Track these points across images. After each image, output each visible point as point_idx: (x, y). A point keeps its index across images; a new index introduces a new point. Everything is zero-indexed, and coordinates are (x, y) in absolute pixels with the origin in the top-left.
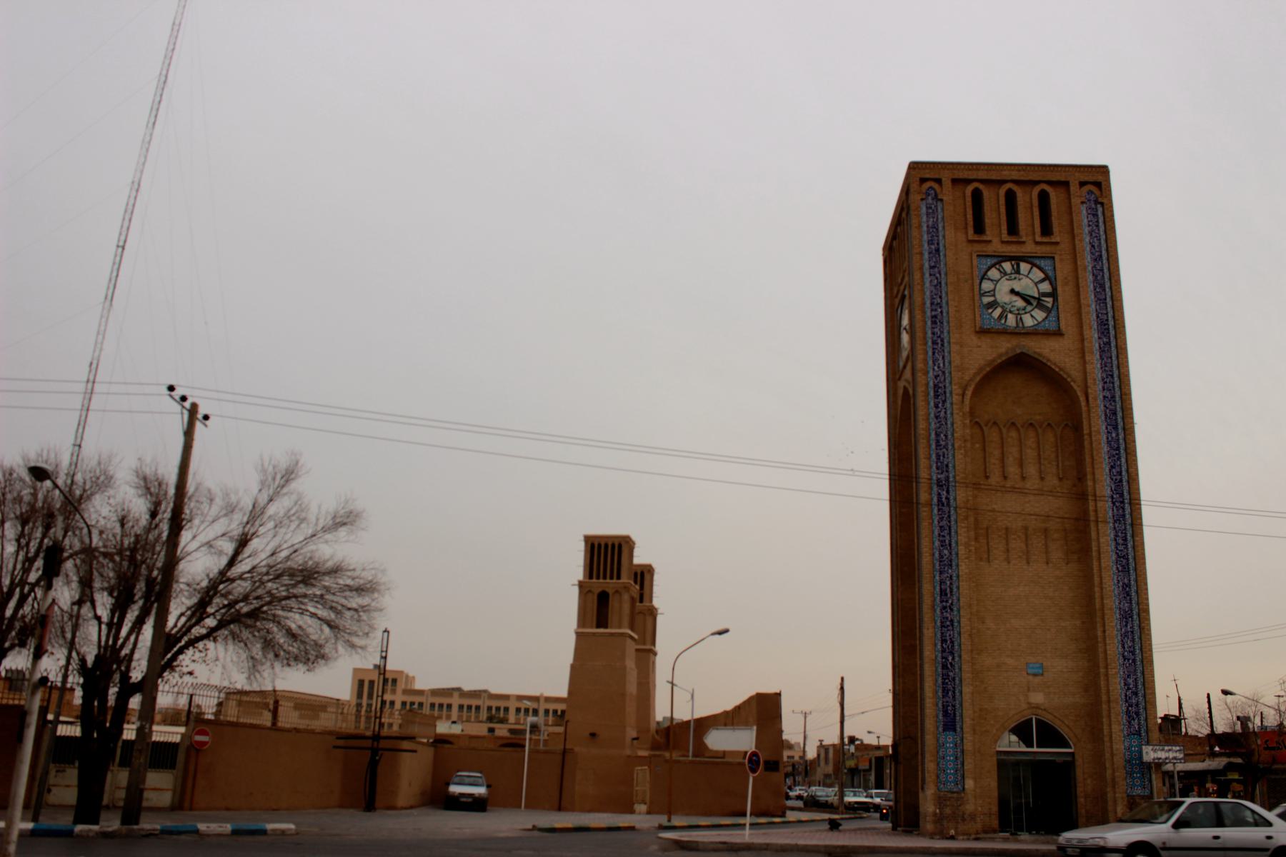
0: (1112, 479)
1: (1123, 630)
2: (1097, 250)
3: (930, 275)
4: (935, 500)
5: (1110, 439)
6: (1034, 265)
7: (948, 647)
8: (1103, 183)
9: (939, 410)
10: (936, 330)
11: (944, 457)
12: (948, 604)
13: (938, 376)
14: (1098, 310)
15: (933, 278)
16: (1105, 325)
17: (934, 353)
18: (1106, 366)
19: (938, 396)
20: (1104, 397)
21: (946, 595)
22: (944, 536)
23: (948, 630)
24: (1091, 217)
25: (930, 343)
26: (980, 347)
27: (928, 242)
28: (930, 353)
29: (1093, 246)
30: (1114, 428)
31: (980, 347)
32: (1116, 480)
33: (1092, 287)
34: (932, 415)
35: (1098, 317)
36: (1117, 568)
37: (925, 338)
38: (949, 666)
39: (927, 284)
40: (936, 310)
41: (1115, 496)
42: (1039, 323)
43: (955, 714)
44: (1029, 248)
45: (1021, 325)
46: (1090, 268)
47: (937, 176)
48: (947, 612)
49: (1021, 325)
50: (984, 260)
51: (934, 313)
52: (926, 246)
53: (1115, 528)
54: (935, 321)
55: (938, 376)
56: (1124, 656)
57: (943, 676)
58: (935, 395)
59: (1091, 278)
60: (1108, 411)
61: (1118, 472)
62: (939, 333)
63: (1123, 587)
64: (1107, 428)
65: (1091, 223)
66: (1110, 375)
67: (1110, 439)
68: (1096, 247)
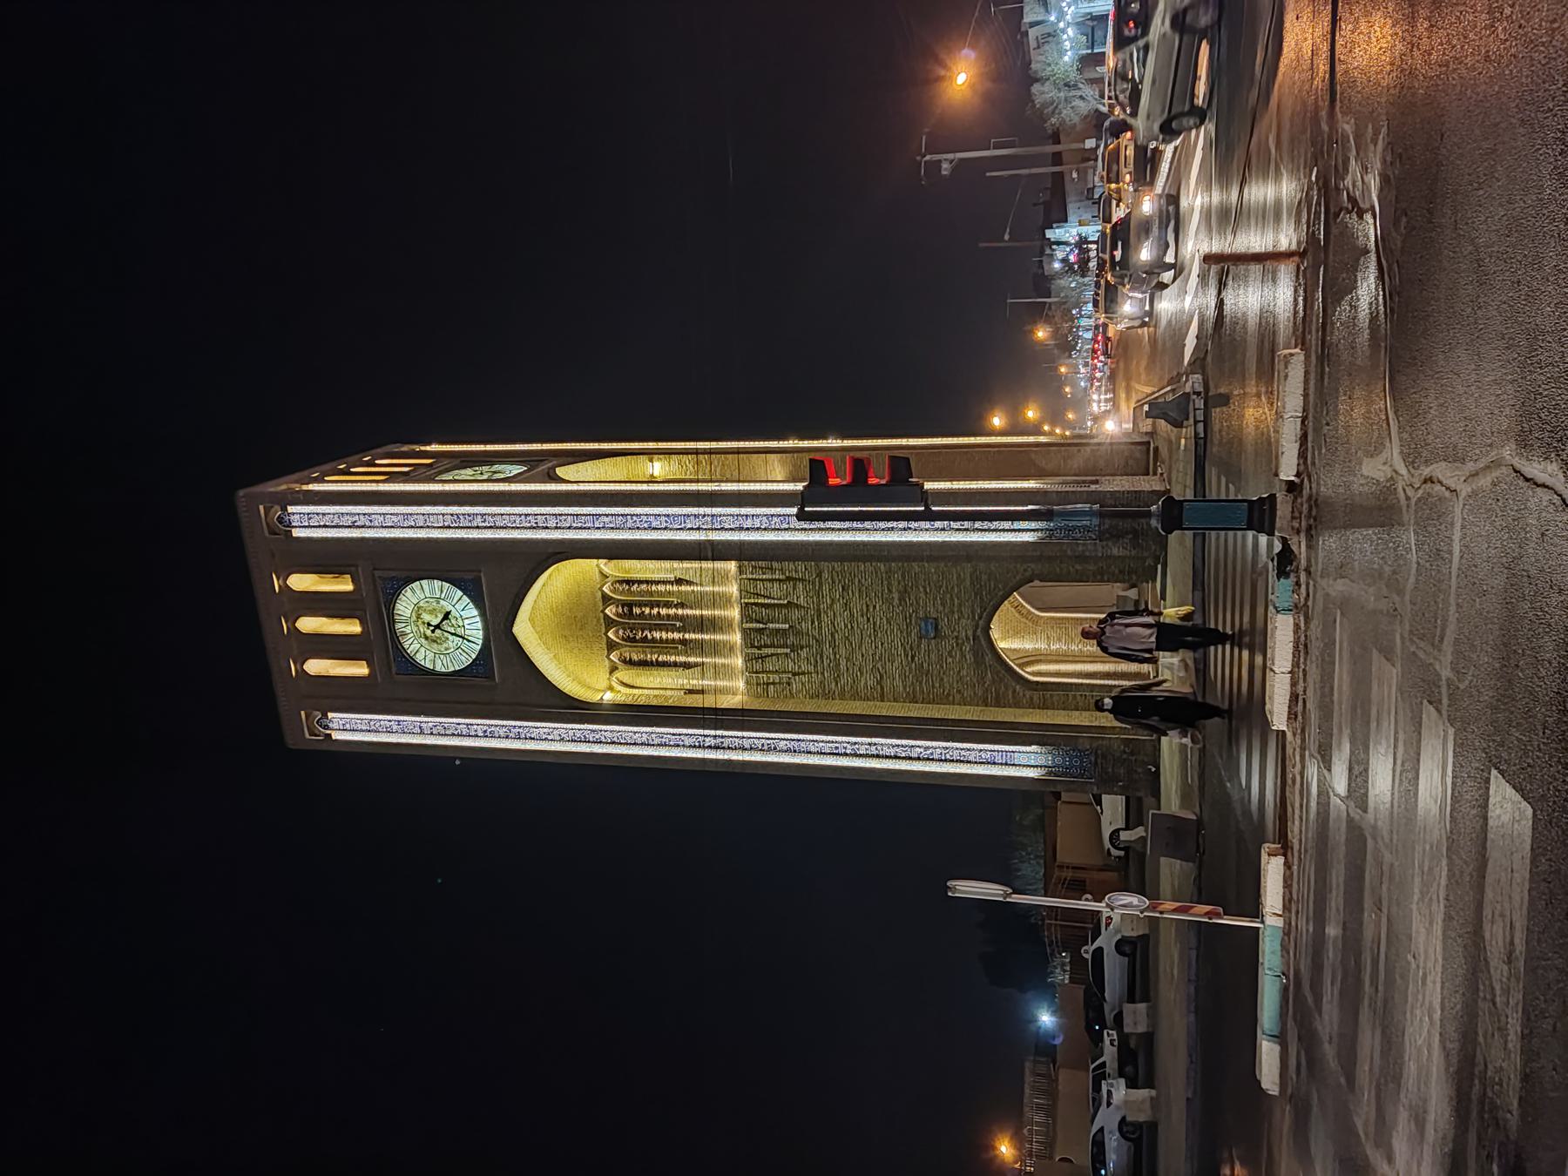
11: (662, 737)
16: (458, 517)
18: (515, 522)
30: (597, 519)
32: (666, 522)
68: (354, 519)
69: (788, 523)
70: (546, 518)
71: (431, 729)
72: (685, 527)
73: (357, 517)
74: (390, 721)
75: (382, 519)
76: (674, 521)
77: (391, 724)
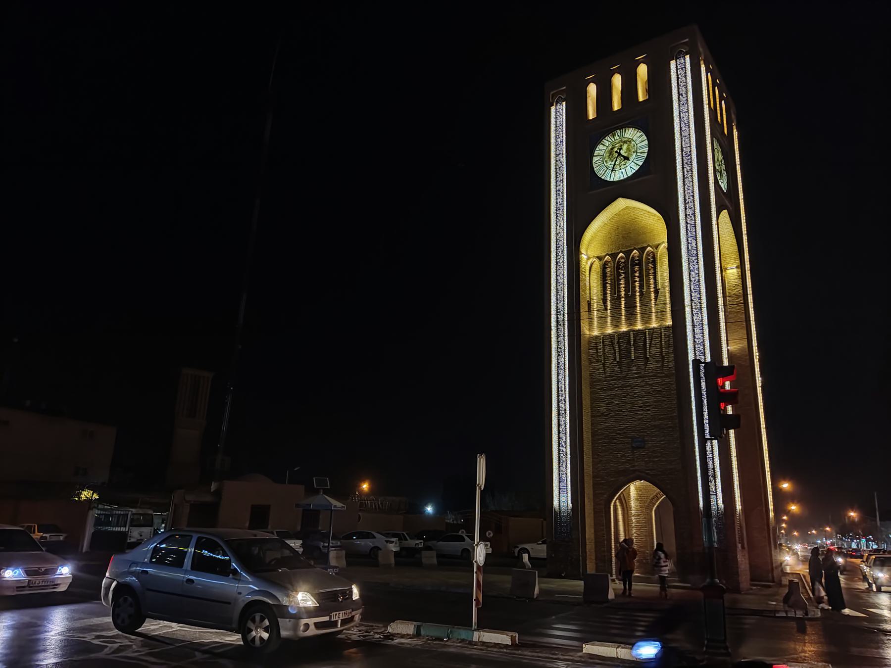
11: (561, 291)
16: (689, 155)
18: (688, 190)
30: (693, 239)
32: (695, 281)
43: (567, 480)
54: (559, 193)
61: (697, 274)
62: (561, 202)
68: (684, 94)
69: (699, 355)
70: (692, 208)
71: (559, 160)
72: (692, 292)
74: (562, 137)
75: (685, 111)
76: (696, 285)
77: (561, 137)
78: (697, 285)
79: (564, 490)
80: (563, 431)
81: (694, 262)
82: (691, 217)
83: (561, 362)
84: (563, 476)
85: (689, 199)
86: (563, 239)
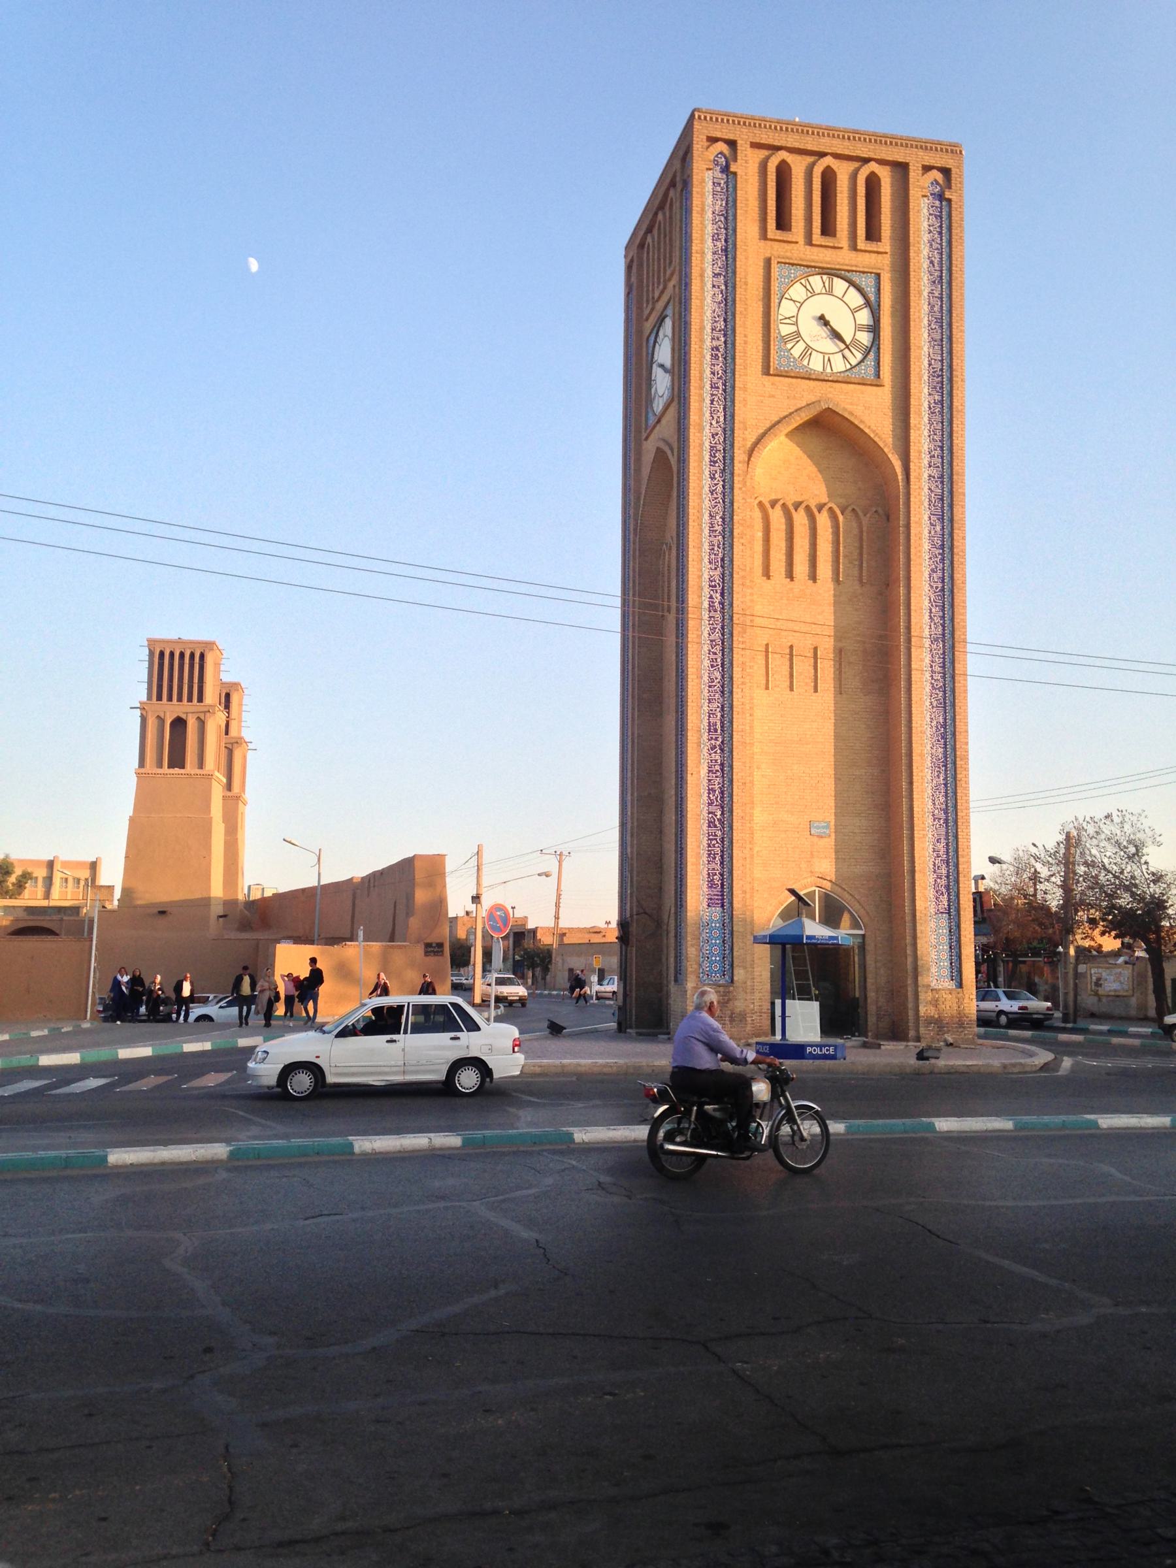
0: (932, 587)
1: (935, 782)
2: (938, 268)
3: (714, 286)
4: (706, 605)
5: (933, 532)
6: (851, 283)
7: (716, 798)
8: (954, 171)
9: (716, 482)
10: (717, 368)
11: (719, 547)
12: (718, 743)
13: (717, 434)
14: (931, 355)
15: (716, 290)
16: (938, 376)
17: (712, 401)
18: (935, 434)
19: (715, 462)
20: (930, 476)
21: (716, 730)
22: (715, 654)
23: (716, 777)
24: (933, 220)
25: (708, 386)
26: (773, 396)
27: (713, 236)
28: (708, 401)
29: (932, 262)
30: (938, 519)
31: (773, 396)
32: (937, 588)
33: (926, 322)
34: (706, 489)
35: (930, 365)
36: (931, 703)
37: (701, 379)
38: (717, 823)
39: (709, 300)
40: (718, 339)
41: (933, 610)
42: (853, 367)
44: (845, 258)
45: (828, 370)
46: (925, 294)
47: (731, 137)
48: (716, 752)
49: (828, 370)
50: (786, 270)
51: (715, 343)
52: (709, 242)
53: (931, 650)
54: (717, 355)
55: (717, 434)
56: (933, 815)
57: (709, 836)
58: (711, 461)
59: (926, 308)
60: (933, 495)
63: (937, 727)
64: (930, 518)
65: (931, 228)
66: (939, 446)
67: (933, 532)
68: (936, 265)
69: (937, 707)
70: (938, 467)
72: (932, 605)
73: (938, 268)
75: (937, 295)
78: (940, 595)
79: (717, 901)
80: (717, 801)
81: (937, 557)
82: (936, 482)
83: (716, 679)
84: (715, 877)
85: (935, 450)
86: (724, 449)
